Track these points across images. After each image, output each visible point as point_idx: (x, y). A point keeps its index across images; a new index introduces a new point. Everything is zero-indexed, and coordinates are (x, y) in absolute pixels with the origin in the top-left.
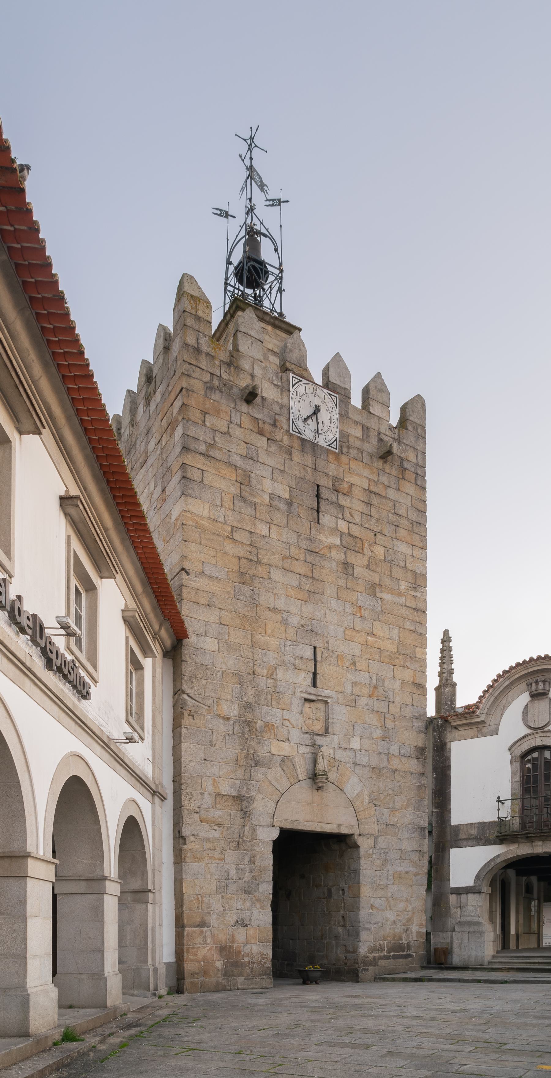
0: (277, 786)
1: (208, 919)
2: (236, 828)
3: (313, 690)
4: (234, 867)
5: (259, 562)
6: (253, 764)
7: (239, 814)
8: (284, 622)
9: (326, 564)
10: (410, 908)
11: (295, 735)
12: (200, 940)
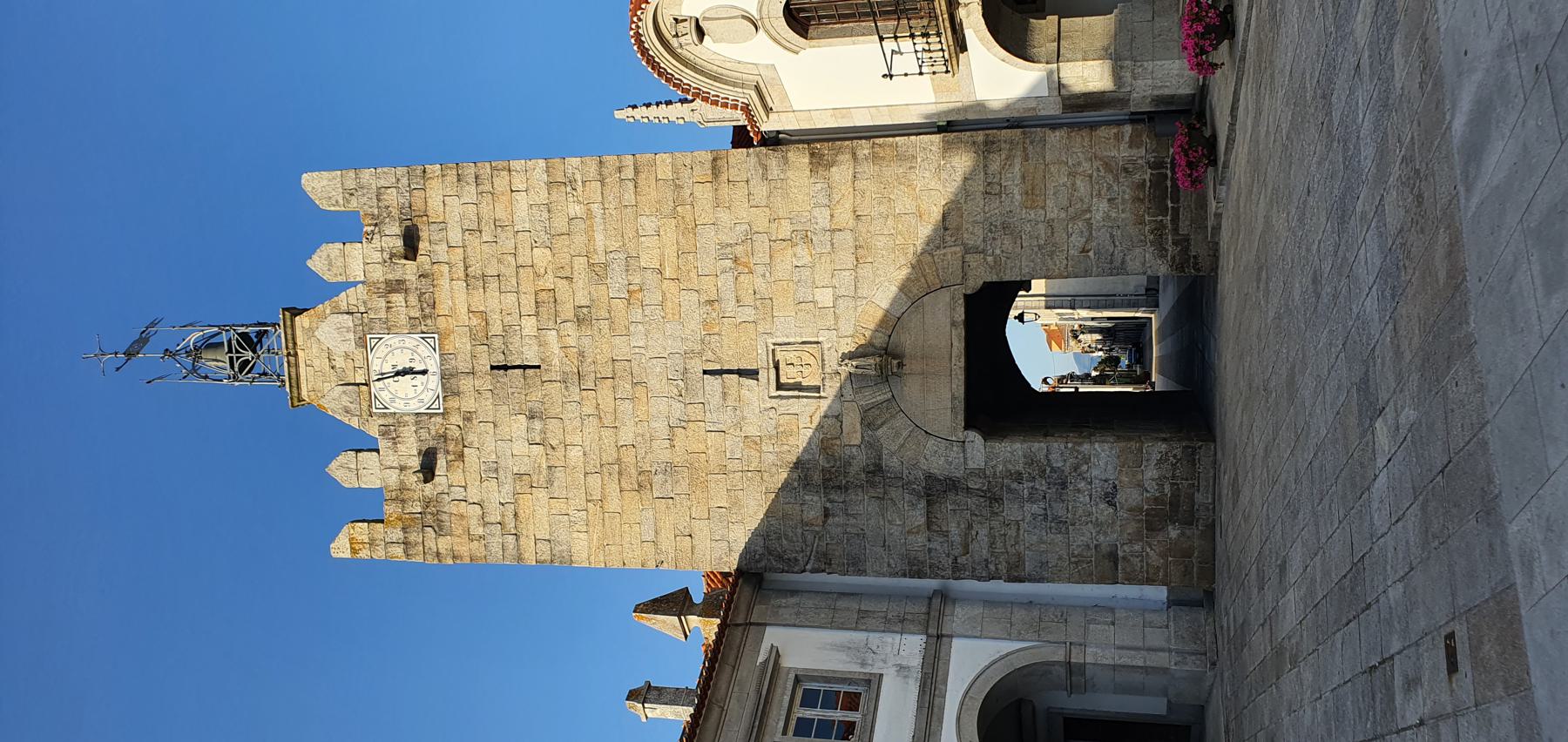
0: (905, 434)
1: (1105, 549)
2: (971, 502)
3: (762, 375)
4: (1027, 506)
5: (619, 461)
7: (951, 496)
8: (684, 423)
10: (1086, 165)
12: (1136, 561)
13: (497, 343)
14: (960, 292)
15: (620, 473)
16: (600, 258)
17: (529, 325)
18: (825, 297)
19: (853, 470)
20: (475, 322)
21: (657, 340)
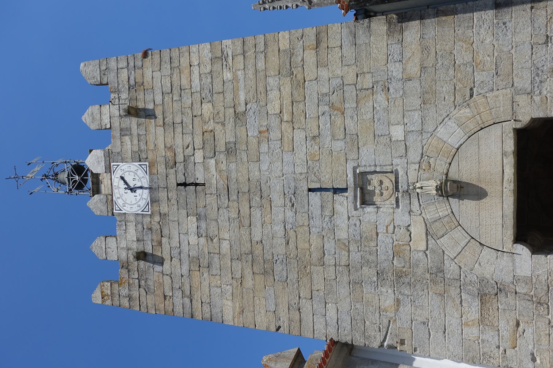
6: (441, 275)
9: (233, 175)
11: (401, 217)
13: (180, 167)
14: (509, 127)
15: (253, 261)
16: (241, 109)
17: (199, 156)
18: (398, 132)
19: (419, 271)
20: (169, 154)
21: (278, 167)
